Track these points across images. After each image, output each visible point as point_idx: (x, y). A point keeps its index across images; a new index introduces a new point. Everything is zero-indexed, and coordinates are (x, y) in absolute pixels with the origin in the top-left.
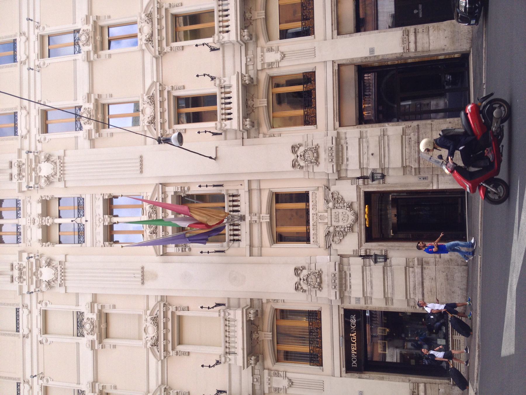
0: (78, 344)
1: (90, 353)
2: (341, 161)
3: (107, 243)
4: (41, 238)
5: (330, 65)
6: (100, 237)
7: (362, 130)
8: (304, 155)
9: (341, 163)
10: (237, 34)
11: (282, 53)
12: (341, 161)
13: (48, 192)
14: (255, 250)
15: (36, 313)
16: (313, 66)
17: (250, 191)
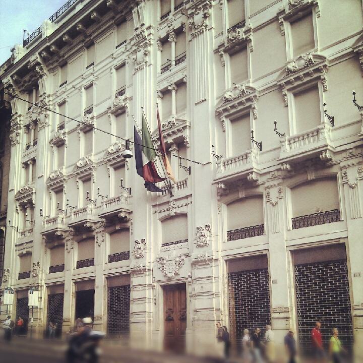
0: (110, 98)
1: (105, 109)
2: (201, 264)
3: (159, 94)
4: (162, 37)
5: (266, 247)
6: (162, 87)
7: (221, 280)
8: (202, 235)
9: (200, 264)
10: (305, 153)
11: (277, 203)
12: (201, 264)
13: (186, 30)
14: (157, 209)
15: (124, 57)
16: (266, 234)
17: (187, 197)
